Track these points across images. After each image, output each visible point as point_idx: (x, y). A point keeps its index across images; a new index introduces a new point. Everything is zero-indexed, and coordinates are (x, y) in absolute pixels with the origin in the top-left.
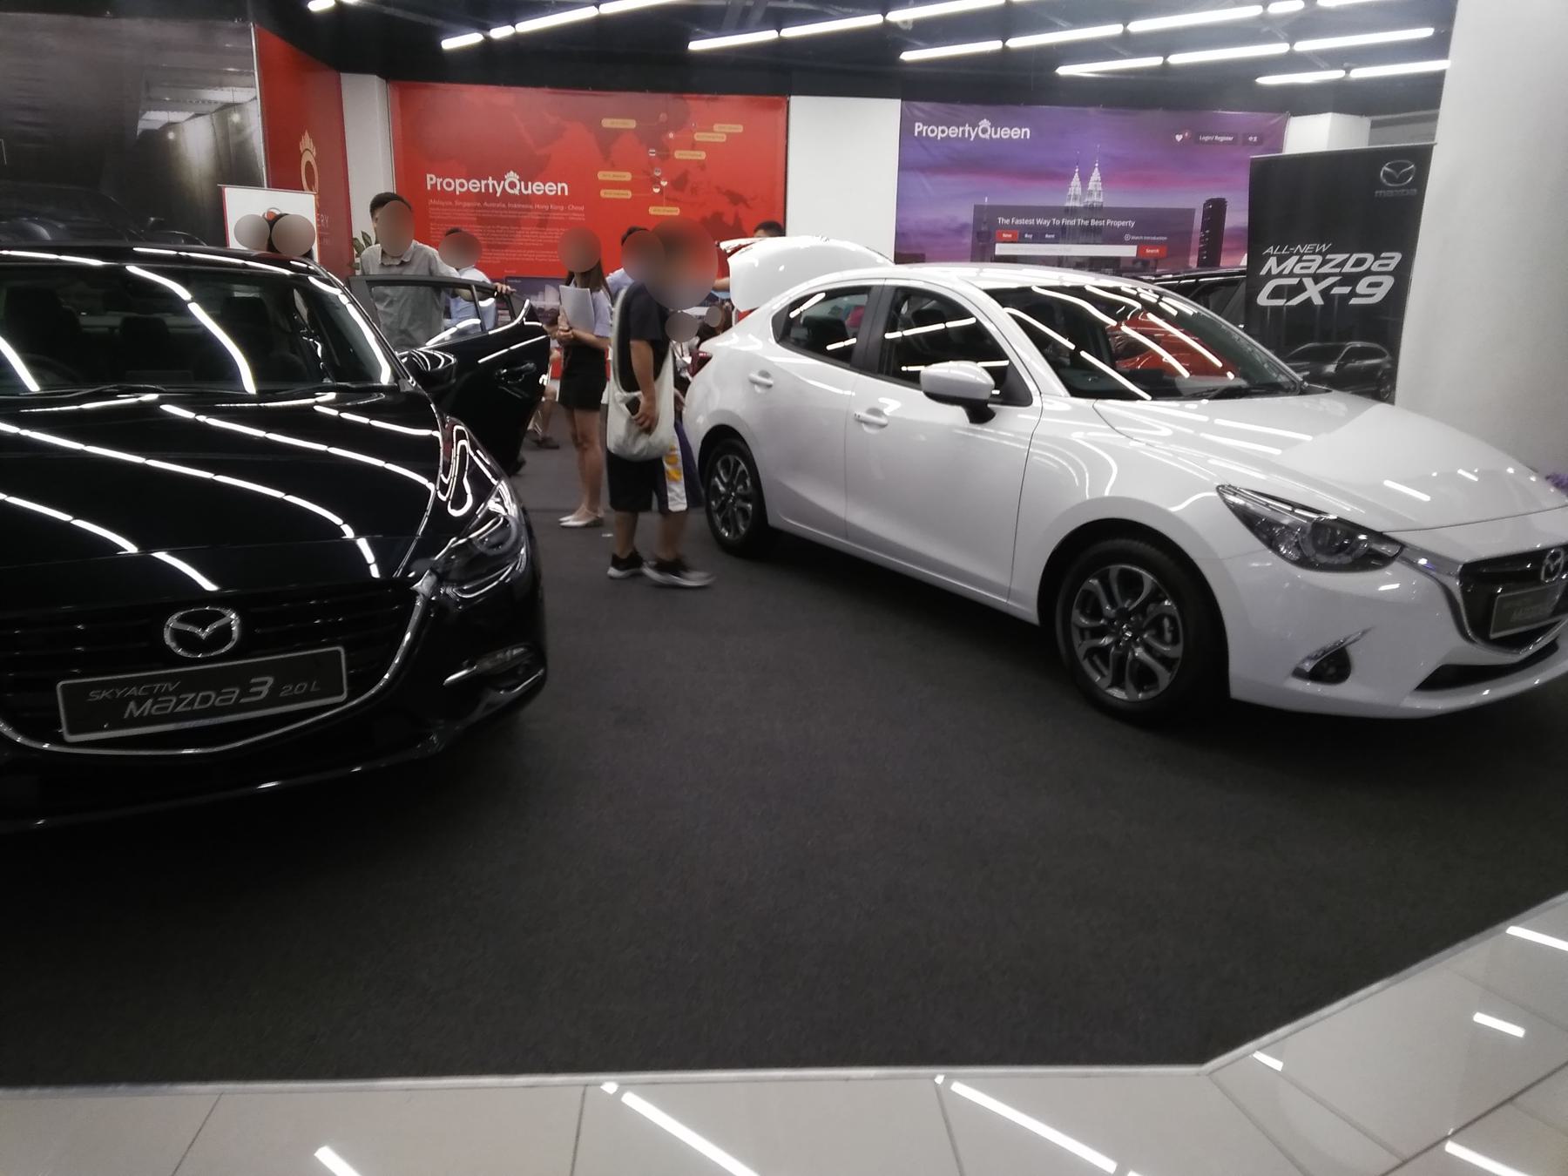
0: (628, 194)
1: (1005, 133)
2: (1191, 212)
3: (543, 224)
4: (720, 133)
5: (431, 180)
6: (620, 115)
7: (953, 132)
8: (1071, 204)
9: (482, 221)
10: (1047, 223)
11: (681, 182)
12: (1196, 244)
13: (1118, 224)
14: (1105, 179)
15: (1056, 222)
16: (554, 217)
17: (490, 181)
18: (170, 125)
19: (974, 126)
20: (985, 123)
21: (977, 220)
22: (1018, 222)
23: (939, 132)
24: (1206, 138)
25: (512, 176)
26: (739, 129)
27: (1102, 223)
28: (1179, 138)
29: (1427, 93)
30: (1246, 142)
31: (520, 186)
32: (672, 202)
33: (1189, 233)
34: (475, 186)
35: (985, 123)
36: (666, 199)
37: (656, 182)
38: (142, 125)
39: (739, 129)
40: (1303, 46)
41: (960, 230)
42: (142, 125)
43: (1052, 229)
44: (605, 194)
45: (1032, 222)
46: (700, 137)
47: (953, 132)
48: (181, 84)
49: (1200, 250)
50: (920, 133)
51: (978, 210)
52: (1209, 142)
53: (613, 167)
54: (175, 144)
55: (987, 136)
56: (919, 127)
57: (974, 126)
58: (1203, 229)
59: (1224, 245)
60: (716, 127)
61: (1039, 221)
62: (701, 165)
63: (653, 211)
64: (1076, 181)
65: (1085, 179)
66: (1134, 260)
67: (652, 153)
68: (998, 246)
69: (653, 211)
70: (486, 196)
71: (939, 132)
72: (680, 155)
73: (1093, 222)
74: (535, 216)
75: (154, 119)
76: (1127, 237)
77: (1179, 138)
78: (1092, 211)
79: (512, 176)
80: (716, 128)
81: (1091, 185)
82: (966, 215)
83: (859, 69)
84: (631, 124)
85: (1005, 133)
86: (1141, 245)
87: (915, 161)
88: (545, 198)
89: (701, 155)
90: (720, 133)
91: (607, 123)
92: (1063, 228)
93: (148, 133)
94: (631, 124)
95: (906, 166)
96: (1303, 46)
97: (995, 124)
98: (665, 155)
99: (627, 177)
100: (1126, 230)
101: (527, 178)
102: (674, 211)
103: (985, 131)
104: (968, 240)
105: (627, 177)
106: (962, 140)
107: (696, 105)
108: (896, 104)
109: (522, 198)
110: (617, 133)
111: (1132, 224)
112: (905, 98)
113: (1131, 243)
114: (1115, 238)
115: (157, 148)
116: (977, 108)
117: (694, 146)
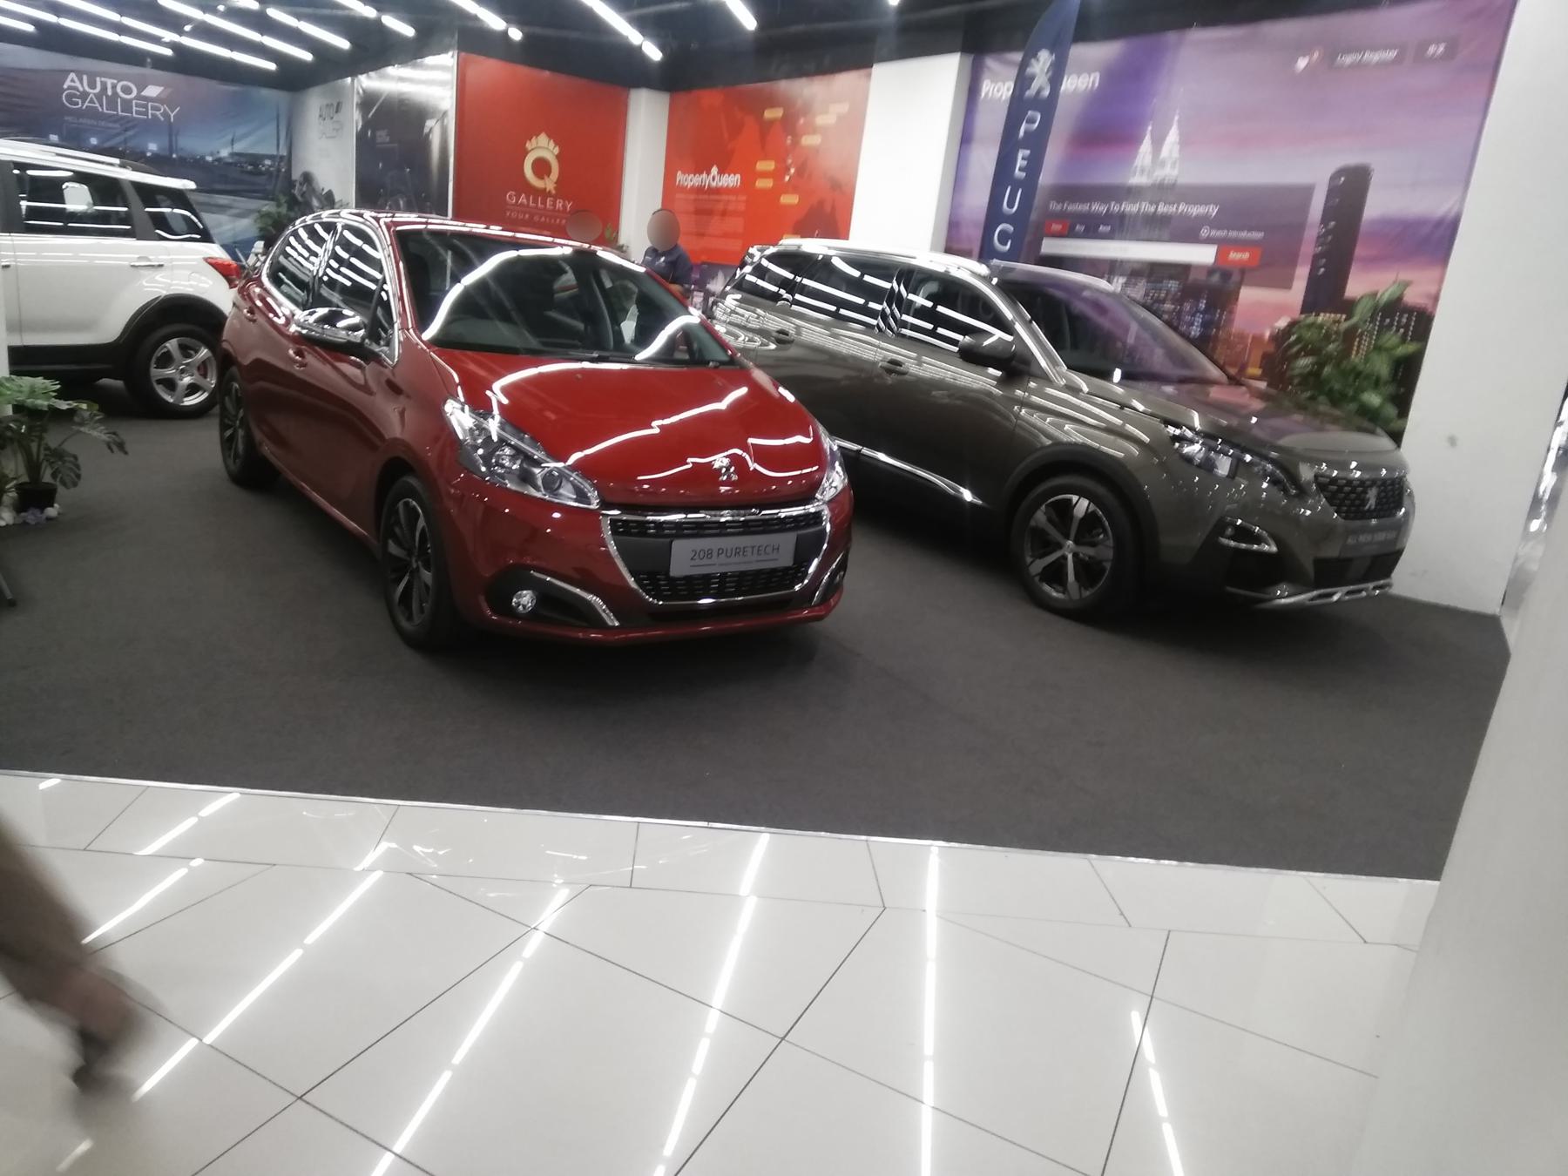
2: (1308, 191)
3: (724, 214)
5: (680, 176)
8: (1137, 180)
12: (1308, 248)
13: (1196, 211)
14: (1184, 142)
16: (731, 207)
24: (1348, 59)
25: (714, 170)
27: (1172, 209)
28: (1302, 63)
33: (1301, 227)
49: (1316, 258)
52: (1358, 66)
53: (766, 158)
58: (1325, 220)
59: (1359, 251)
64: (1146, 146)
65: (1158, 143)
66: (1211, 270)
70: (699, 190)
73: (1162, 209)
74: (721, 207)
76: (1204, 233)
78: (1163, 191)
79: (714, 170)
81: (1165, 152)
86: (1224, 245)
92: (1122, 217)
100: (1203, 220)
101: (721, 172)
111: (1213, 210)
112: (965, 49)
113: (1209, 241)
114: (1187, 233)
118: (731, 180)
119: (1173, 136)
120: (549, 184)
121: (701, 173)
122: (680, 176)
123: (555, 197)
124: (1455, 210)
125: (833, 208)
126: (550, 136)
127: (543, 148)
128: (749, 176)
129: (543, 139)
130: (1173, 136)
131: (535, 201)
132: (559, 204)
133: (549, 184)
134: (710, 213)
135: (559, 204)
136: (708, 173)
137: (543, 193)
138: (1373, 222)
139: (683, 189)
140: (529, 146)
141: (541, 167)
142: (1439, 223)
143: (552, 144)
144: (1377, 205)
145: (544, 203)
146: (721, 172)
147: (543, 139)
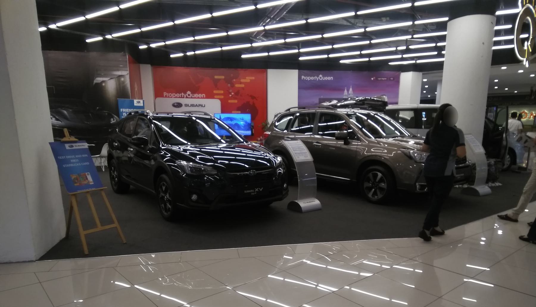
4: (248, 79)
6: (219, 75)
7: (312, 78)
8: (345, 97)
11: (237, 93)
14: (353, 90)
18: (103, 82)
19: (318, 76)
20: (321, 76)
23: (309, 78)
26: (253, 78)
28: (372, 79)
29: (439, 66)
30: (390, 80)
32: (235, 99)
35: (321, 76)
36: (233, 98)
37: (230, 93)
38: (95, 82)
39: (253, 78)
40: (405, 56)
42: (95, 82)
46: (242, 80)
47: (312, 78)
48: (107, 71)
53: (218, 89)
54: (104, 87)
56: (303, 77)
57: (318, 76)
60: (247, 78)
62: (243, 88)
63: (230, 101)
64: (346, 91)
65: (348, 90)
67: (229, 85)
69: (230, 101)
71: (309, 78)
72: (237, 86)
75: (99, 80)
77: (372, 79)
80: (247, 79)
81: (350, 92)
83: (288, 63)
84: (223, 77)
87: (303, 86)
89: (243, 86)
90: (248, 79)
91: (216, 77)
93: (97, 84)
94: (223, 77)
95: (300, 88)
96: (405, 56)
97: (324, 76)
98: (233, 86)
99: (222, 92)
102: (236, 101)
105: (222, 92)
106: (315, 80)
107: (241, 72)
108: (297, 70)
110: (219, 80)
115: (100, 88)
116: (318, 72)
117: (241, 83)
119: (351, 89)
125: (254, 103)
130: (351, 89)
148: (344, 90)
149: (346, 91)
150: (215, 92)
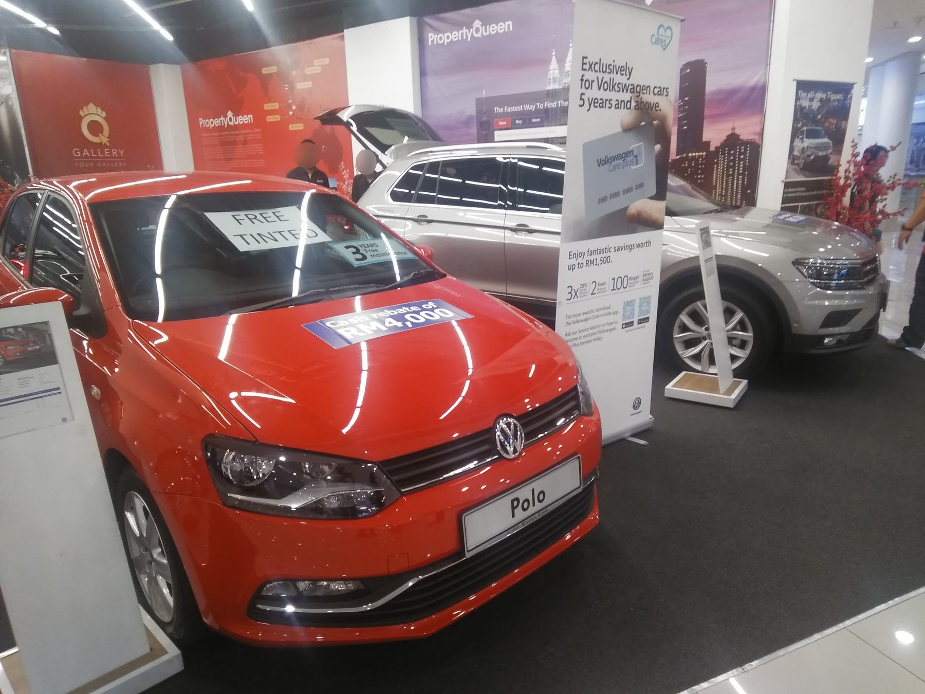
0: (277, 118)
1: (493, 29)
3: (245, 142)
5: (202, 121)
7: (455, 36)
8: (551, 87)
9: (223, 144)
10: (532, 108)
15: (540, 106)
17: (222, 119)
19: (469, 27)
20: (477, 24)
21: (479, 112)
22: (510, 110)
25: (230, 114)
31: (233, 119)
34: (216, 122)
35: (477, 24)
41: (467, 122)
43: (537, 113)
44: (270, 119)
45: (520, 108)
46: (309, 71)
50: (433, 41)
51: (479, 102)
53: (270, 101)
55: (479, 35)
57: (469, 27)
61: (527, 107)
64: (554, 64)
65: (561, 61)
68: (496, 133)
70: (221, 128)
74: (241, 138)
79: (230, 114)
81: (568, 66)
82: (470, 109)
85: (493, 29)
88: (244, 126)
89: (308, 85)
92: (547, 111)
101: (236, 114)
103: (477, 30)
104: (474, 130)
106: (463, 41)
109: (236, 127)
117: (306, 78)
118: (246, 119)
120: (104, 139)
121: (219, 117)
122: (202, 121)
123: (110, 148)
124: (762, 80)
126: (97, 106)
127: (93, 113)
128: (260, 115)
129: (92, 108)
131: (96, 153)
132: (114, 153)
133: (104, 139)
134: (234, 143)
135: (114, 153)
136: (225, 117)
137: (100, 145)
138: (713, 93)
139: (208, 130)
140: (81, 113)
141: (95, 127)
142: (753, 89)
143: (99, 110)
144: (714, 83)
145: (103, 153)
146: (236, 114)
147: (92, 108)
148: (548, 62)
149: (554, 64)
150: (267, 107)
